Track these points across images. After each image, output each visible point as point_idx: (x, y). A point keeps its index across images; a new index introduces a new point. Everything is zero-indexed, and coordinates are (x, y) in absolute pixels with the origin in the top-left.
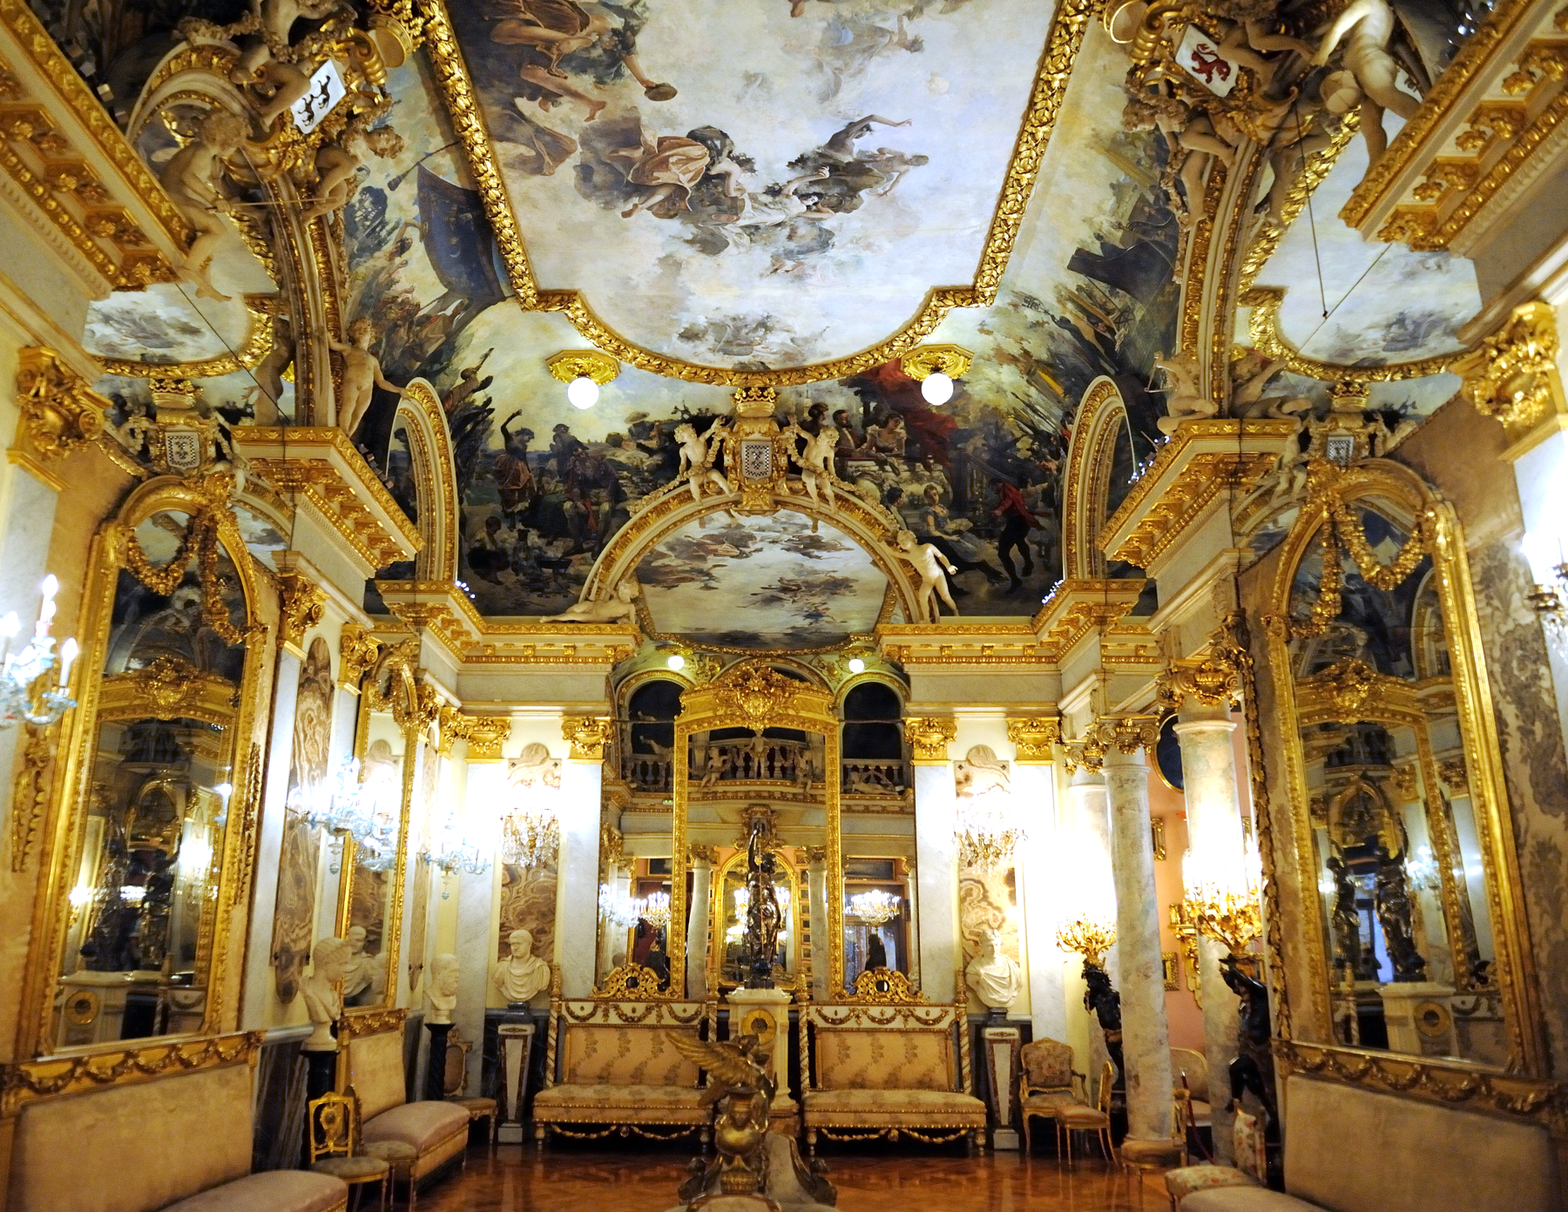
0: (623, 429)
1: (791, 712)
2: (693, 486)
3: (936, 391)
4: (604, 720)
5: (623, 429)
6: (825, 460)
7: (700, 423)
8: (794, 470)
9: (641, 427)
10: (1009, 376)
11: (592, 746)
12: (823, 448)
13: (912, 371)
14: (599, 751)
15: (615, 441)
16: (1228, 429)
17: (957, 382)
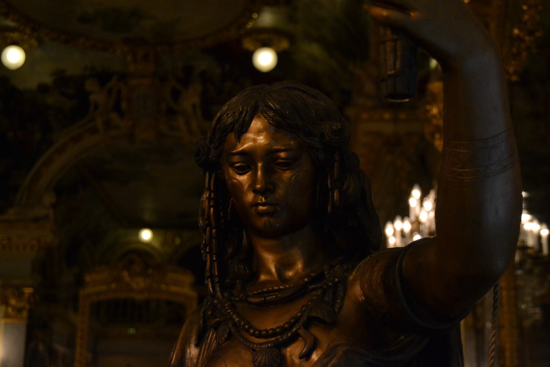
0: (48, 80)
1: (163, 287)
2: (99, 122)
3: (265, 59)
4: (28, 291)
5: (48, 80)
6: (194, 106)
7: (103, 77)
8: (171, 112)
9: (61, 80)
10: (315, 49)
11: (19, 310)
12: (191, 99)
13: (247, 44)
14: (25, 314)
15: (43, 88)
16: (387, 116)
17: (281, 56)
